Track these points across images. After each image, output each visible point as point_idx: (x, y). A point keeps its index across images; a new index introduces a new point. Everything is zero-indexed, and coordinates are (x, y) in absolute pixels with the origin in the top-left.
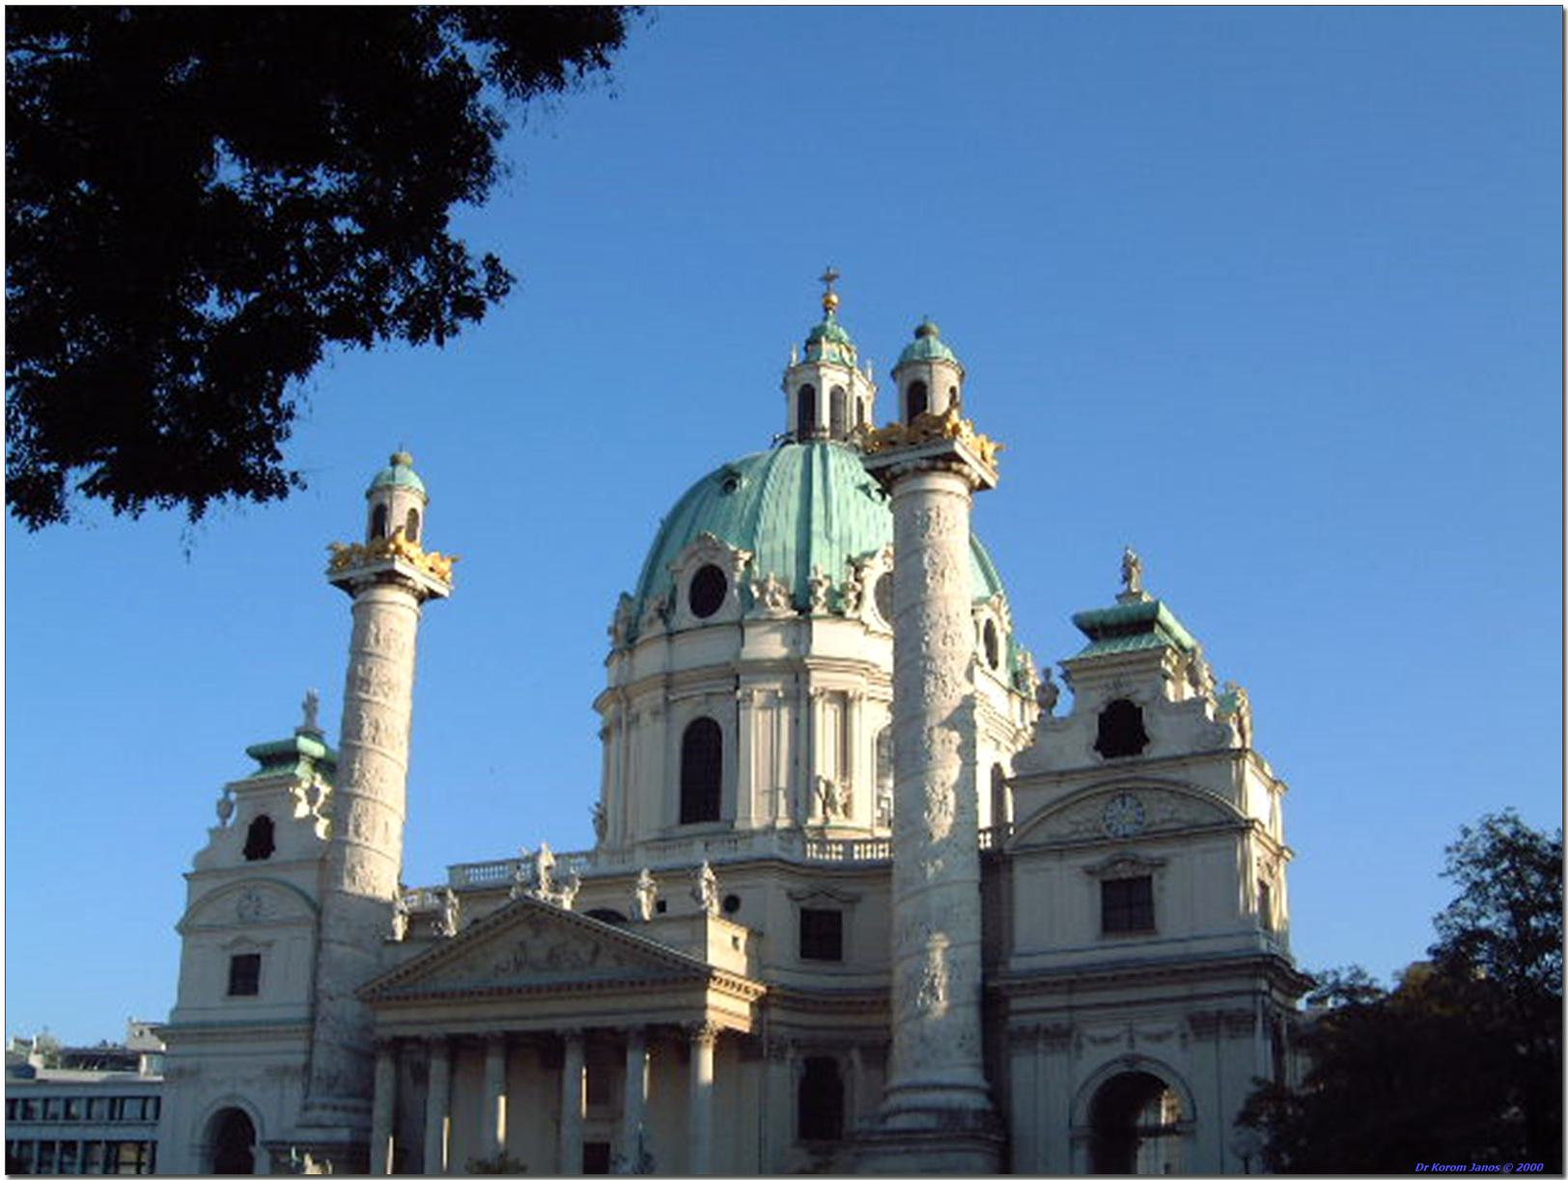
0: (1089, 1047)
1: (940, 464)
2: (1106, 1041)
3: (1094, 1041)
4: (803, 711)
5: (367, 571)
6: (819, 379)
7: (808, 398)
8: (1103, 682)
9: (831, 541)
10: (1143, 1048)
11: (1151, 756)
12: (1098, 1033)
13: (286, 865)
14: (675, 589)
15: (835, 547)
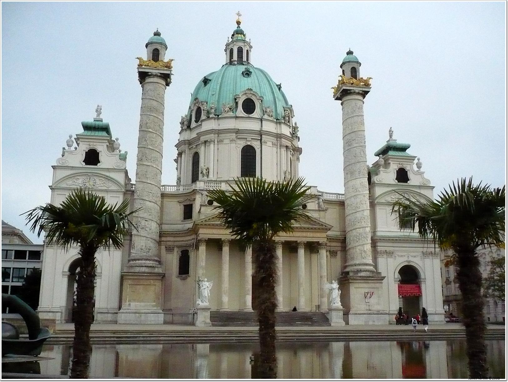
0: (397, 257)
1: (363, 93)
2: (402, 256)
3: (399, 256)
4: (279, 149)
5: (157, 71)
6: (245, 46)
7: (240, 50)
8: (398, 163)
9: (279, 100)
10: (411, 259)
11: (410, 184)
12: (400, 254)
13: (108, 170)
14: (237, 103)
15: (280, 103)
